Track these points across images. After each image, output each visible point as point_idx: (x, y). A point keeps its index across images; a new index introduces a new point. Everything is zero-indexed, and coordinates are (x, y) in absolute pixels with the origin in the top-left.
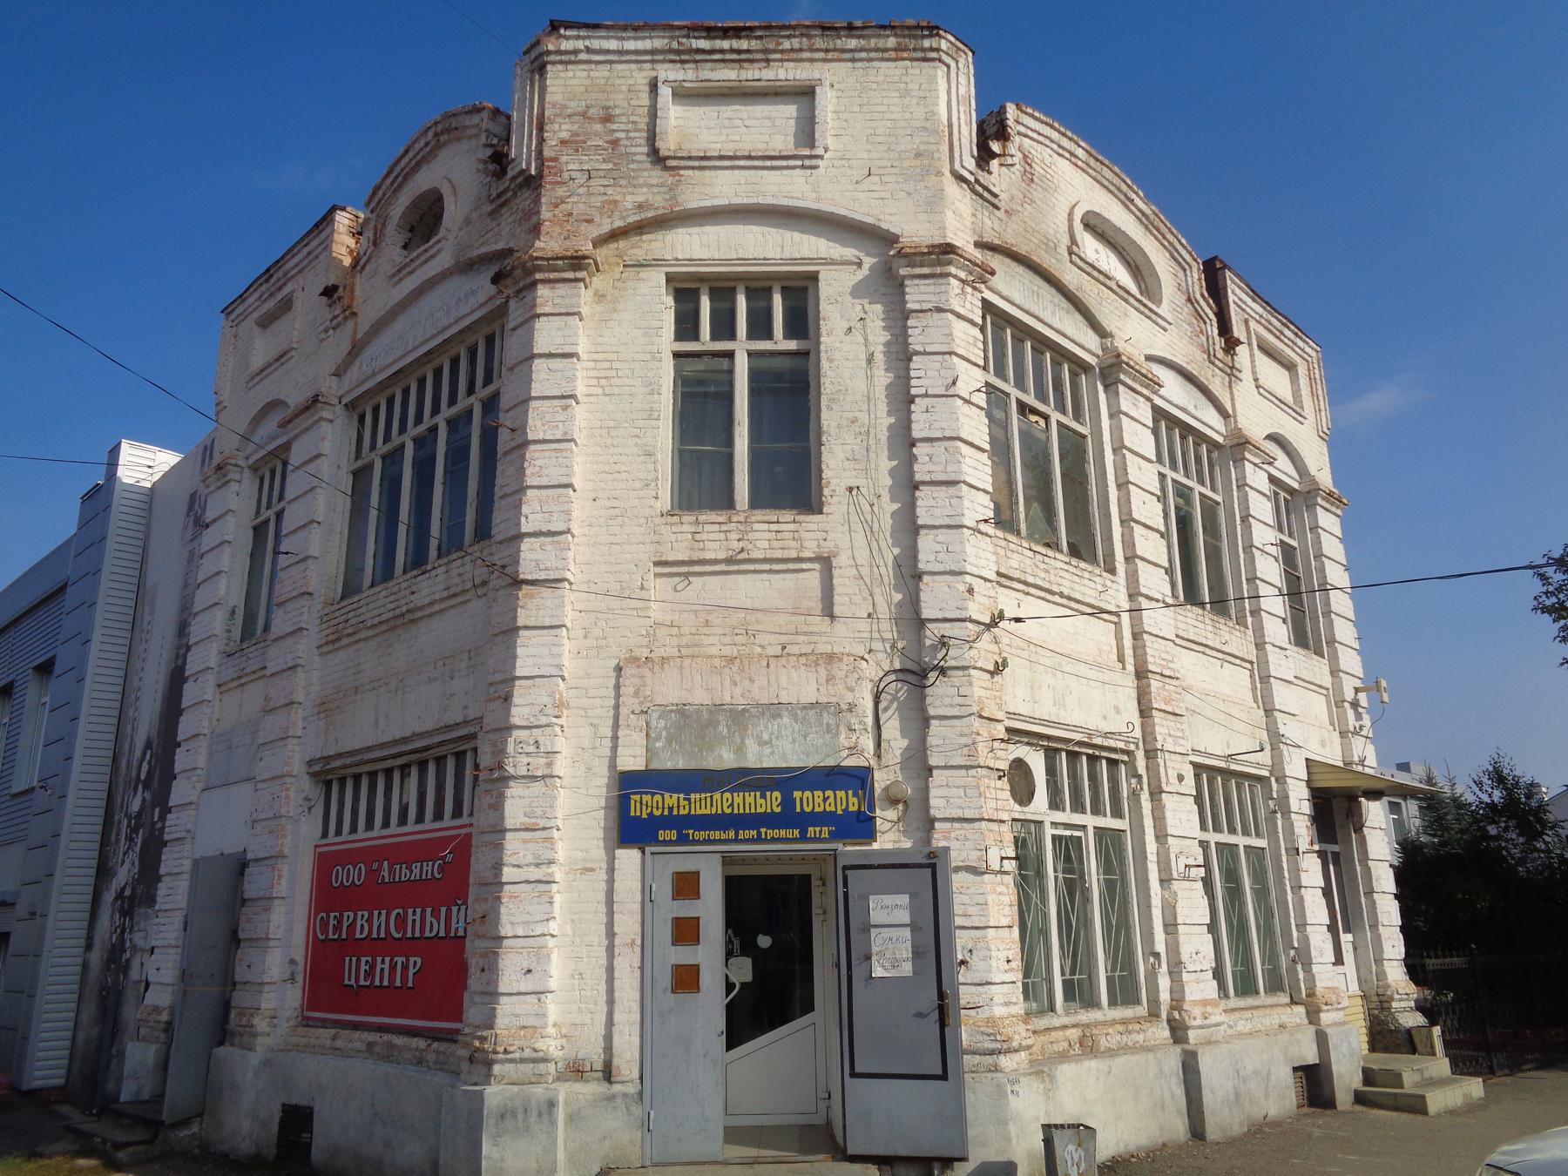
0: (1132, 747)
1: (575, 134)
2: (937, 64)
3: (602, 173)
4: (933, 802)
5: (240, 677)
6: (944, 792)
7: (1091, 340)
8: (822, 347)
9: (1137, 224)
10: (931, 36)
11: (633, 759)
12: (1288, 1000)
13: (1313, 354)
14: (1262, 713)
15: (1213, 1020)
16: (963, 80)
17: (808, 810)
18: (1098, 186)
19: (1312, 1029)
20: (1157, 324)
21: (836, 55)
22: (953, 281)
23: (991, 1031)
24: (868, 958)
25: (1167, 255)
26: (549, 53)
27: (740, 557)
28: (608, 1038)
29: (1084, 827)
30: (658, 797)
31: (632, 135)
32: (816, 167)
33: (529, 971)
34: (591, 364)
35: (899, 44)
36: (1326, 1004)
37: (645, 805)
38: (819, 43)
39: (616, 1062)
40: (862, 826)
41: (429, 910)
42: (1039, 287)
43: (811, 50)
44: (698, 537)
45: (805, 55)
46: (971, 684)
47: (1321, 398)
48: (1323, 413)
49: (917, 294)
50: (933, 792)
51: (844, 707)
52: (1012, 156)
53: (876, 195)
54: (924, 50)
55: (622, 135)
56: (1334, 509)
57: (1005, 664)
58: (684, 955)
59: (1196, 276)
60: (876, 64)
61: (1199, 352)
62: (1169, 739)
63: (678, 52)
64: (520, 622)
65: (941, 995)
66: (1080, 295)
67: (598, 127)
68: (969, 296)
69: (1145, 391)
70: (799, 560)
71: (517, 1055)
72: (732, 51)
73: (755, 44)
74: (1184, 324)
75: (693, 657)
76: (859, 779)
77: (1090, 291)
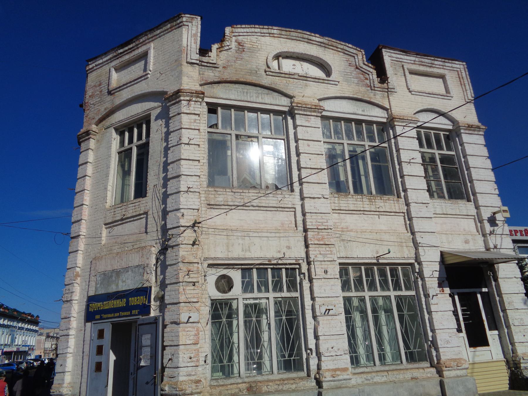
0: (301, 262)
2: (183, 26)
7: (285, 101)
9: (318, 48)
11: (92, 293)
12: (429, 365)
13: (462, 66)
14: (410, 234)
18: (290, 40)
20: (330, 84)
22: (183, 102)
23: (175, 387)
25: (342, 54)
32: (147, 78)
33: (61, 365)
36: (446, 367)
40: (145, 309)
43: (148, 39)
45: (147, 41)
48: (468, 91)
52: (228, 46)
53: (163, 80)
56: (476, 133)
59: (360, 57)
61: (364, 88)
62: (318, 256)
66: (273, 86)
68: (192, 106)
69: (313, 114)
74: (352, 79)
76: (145, 291)
77: (279, 83)
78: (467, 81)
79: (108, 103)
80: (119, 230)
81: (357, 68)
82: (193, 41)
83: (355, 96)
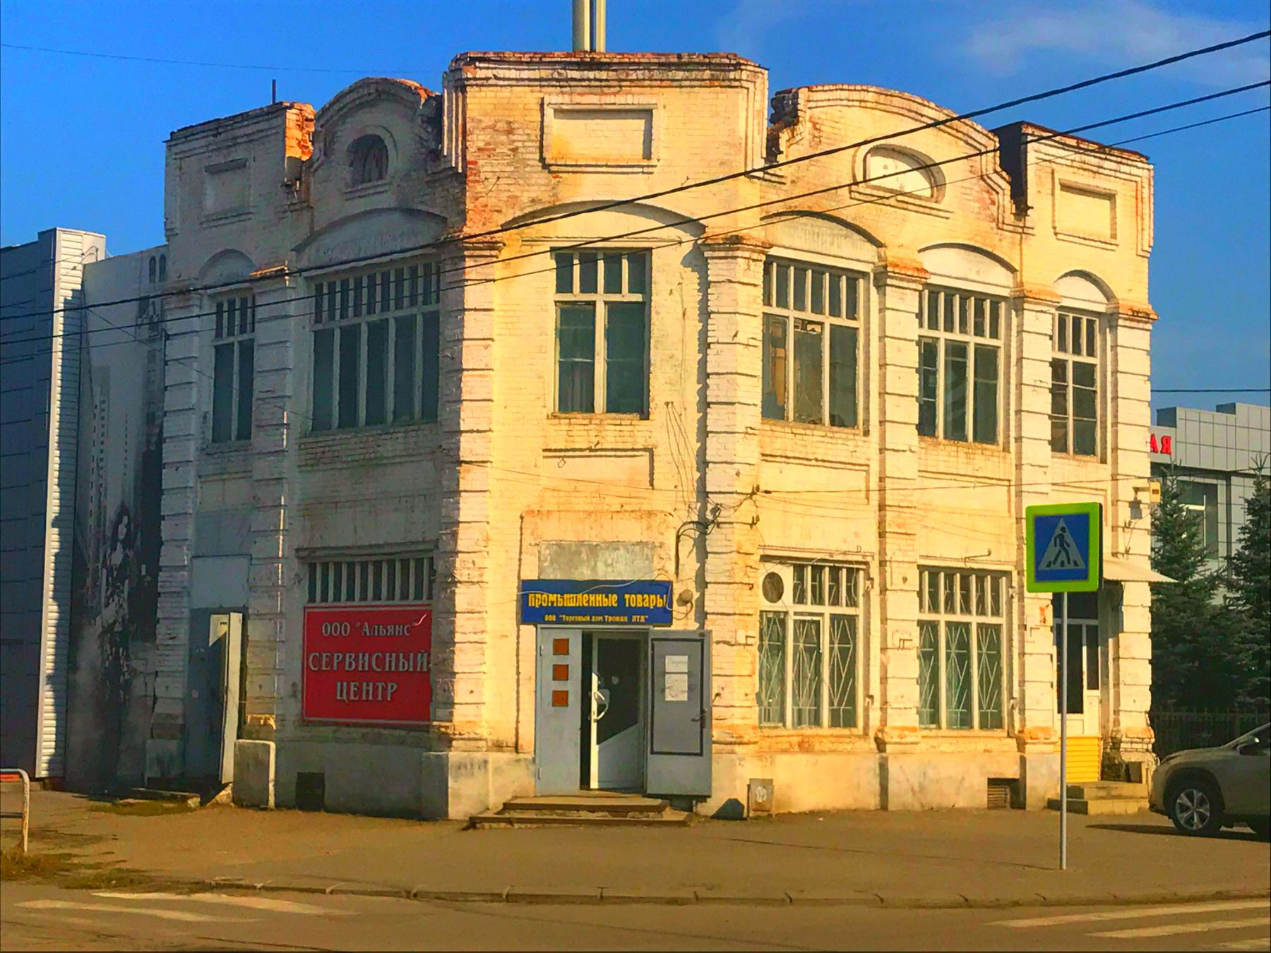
0: (869, 559)
1: (488, 144)
2: (739, 89)
3: (506, 175)
4: (706, 603)
5: (222, 474)
6: (714, 597)
8: (653, 304)
10: (735, 70)
11: (531, 573)
12: (1006, 734)
15: (908, 740)
16: (758, 97)
17: (633, 605)
19: (1019, 754)
21: (669, 83)
24: (663, 690)
25: (962, 143)
26: (468, 79)
27: (598, 447)
28: (517, 729)
29: (821, 615)
30: (545, 596)
31: (526, 144)
32: (651, 173)
33: (472, 692)
34: (502, 313)
35: (712, 75)
37: (536, 600)
38: (656, 74)
39: (520, 742)
40: (665, 616)
41: (401, 655)
42: (820, 227)
43: (650, 80)
44: (570, 433)
45: (647, 83)
46: (733, 533)
47: (1146, 217)
48: (1146, 233)
49: (716, 270)
50: (707, 597)
51: (657, 544)
54: (730, 80)
55: (520, 144)
56: (1141, 325)
57: (758, 519)
58: (559, 686)
60: (697, 89)
63: (557, 80)
64: (461, 488)
65: (702, 711)
67: (503, 138)
70: (633, 450)
71: (466, 736)
72: (596, 80)
73: (612, 75)
75: (567, 511)
76: (664, 588)
78: (1148, 209)
79: (536, 189)
80: (577, 467)
81: (982, 177)
82: (756, 128)
83: (972, 243)
